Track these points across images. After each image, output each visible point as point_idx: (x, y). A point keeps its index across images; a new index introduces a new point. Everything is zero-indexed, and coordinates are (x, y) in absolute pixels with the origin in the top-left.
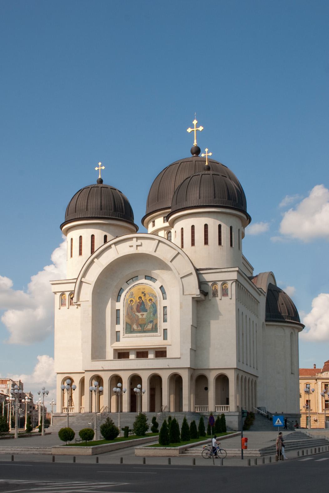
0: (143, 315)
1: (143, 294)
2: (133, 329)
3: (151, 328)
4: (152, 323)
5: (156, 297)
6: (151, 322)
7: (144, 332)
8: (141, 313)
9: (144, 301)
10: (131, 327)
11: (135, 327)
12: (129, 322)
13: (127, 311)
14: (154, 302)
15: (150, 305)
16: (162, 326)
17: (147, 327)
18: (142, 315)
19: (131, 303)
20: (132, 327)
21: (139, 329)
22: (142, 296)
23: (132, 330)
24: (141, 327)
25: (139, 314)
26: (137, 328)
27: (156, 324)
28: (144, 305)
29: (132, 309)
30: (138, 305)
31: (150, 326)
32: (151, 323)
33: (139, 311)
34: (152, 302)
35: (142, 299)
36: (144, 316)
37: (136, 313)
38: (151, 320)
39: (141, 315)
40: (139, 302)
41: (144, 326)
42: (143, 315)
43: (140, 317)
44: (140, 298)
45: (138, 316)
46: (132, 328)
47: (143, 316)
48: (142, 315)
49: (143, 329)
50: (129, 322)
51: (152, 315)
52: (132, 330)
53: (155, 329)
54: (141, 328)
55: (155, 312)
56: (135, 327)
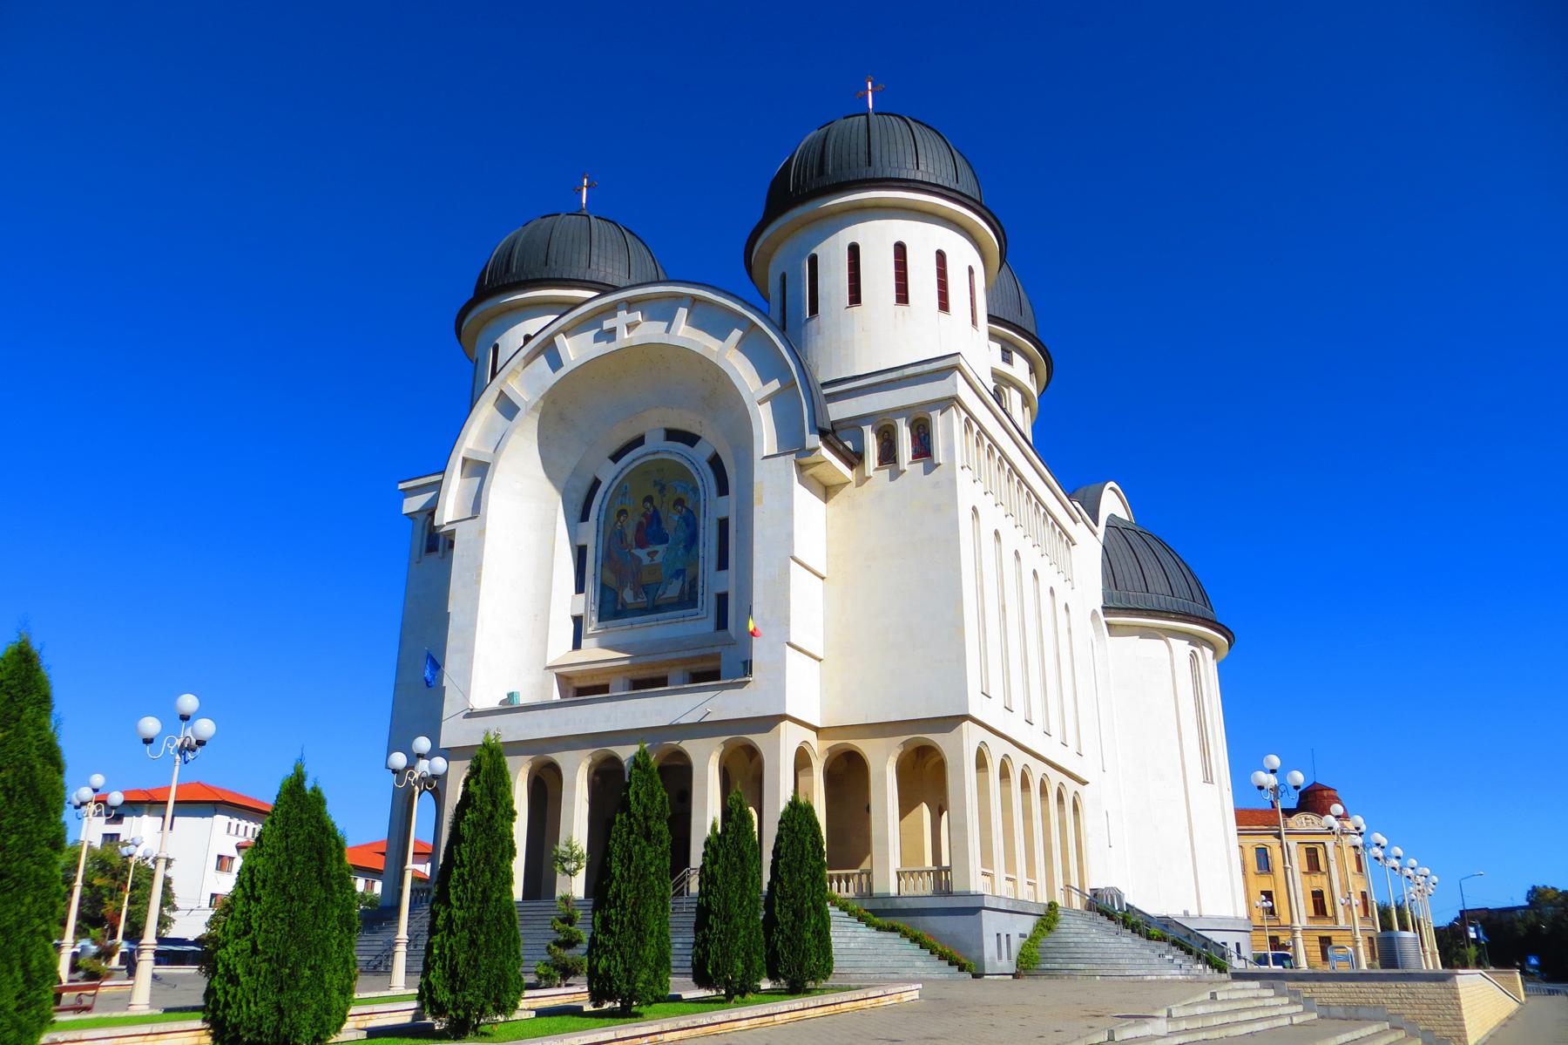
0: (656, 552)
1: (658, 488)
2: (624, 604)
3: (677, 595)
4: (681, 578)
5: (695, 490)
6: (679, 573)
7: (656, 609)
8: (648, 550)
9: (659, 508)
10: (616, 600)
11: (628, 595)
12: (612, 581)
13: (609, 547)
14: (690, 506)
15: (676, 518)
16: (712, 582)
17: (664, 593)
18: (652, 554)
19: (622, 518)
20: (620, 597)
21: (639, 600)
22: (655, 493)
23: (619, 607)
24: (646, 593)
25: (641, 553)
26: (636, 596)
27: (695, 579)
28: (659, 521)
29: (622, 536)
30: (640, 525)
31: (673, 590)
32: (677, 579)
33: (641, 544)
34: (684, 510)
35: (656, 502)
36: (658, 558)
37: (633, 551)
38: (679, 566)
39: (649, 554)
40: (644, 515)
41: (658, 590)
42: (656, 552)
43: (646, 561)
44: (649, 499)
45: (640, 560)
46: (620, 600)
47: (655, 558)
48: (652, 554)
49: (654, 599)
50: (612, 581)
51: (681, 551)
52: (619, 607)
53: (689, 599)
54: (645, 599)
55: (692, 540)
56: (628, 595)
